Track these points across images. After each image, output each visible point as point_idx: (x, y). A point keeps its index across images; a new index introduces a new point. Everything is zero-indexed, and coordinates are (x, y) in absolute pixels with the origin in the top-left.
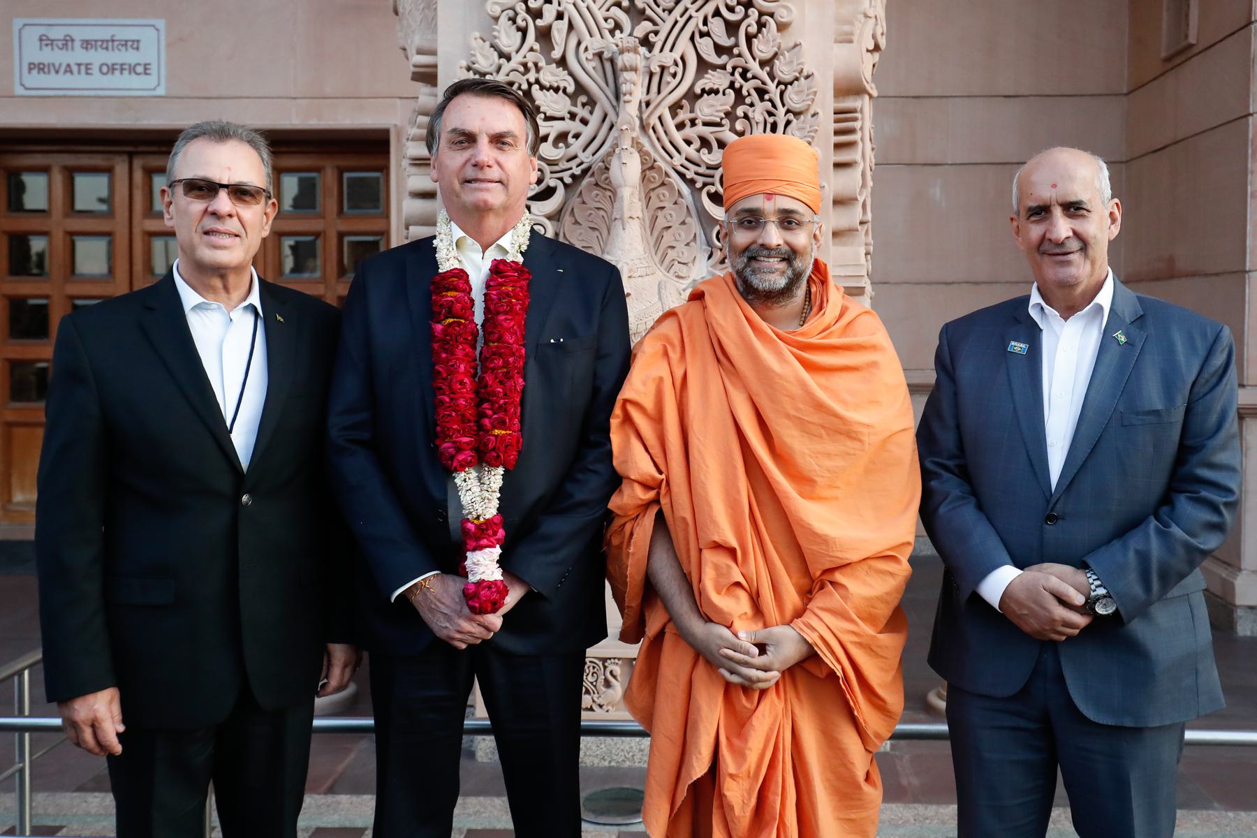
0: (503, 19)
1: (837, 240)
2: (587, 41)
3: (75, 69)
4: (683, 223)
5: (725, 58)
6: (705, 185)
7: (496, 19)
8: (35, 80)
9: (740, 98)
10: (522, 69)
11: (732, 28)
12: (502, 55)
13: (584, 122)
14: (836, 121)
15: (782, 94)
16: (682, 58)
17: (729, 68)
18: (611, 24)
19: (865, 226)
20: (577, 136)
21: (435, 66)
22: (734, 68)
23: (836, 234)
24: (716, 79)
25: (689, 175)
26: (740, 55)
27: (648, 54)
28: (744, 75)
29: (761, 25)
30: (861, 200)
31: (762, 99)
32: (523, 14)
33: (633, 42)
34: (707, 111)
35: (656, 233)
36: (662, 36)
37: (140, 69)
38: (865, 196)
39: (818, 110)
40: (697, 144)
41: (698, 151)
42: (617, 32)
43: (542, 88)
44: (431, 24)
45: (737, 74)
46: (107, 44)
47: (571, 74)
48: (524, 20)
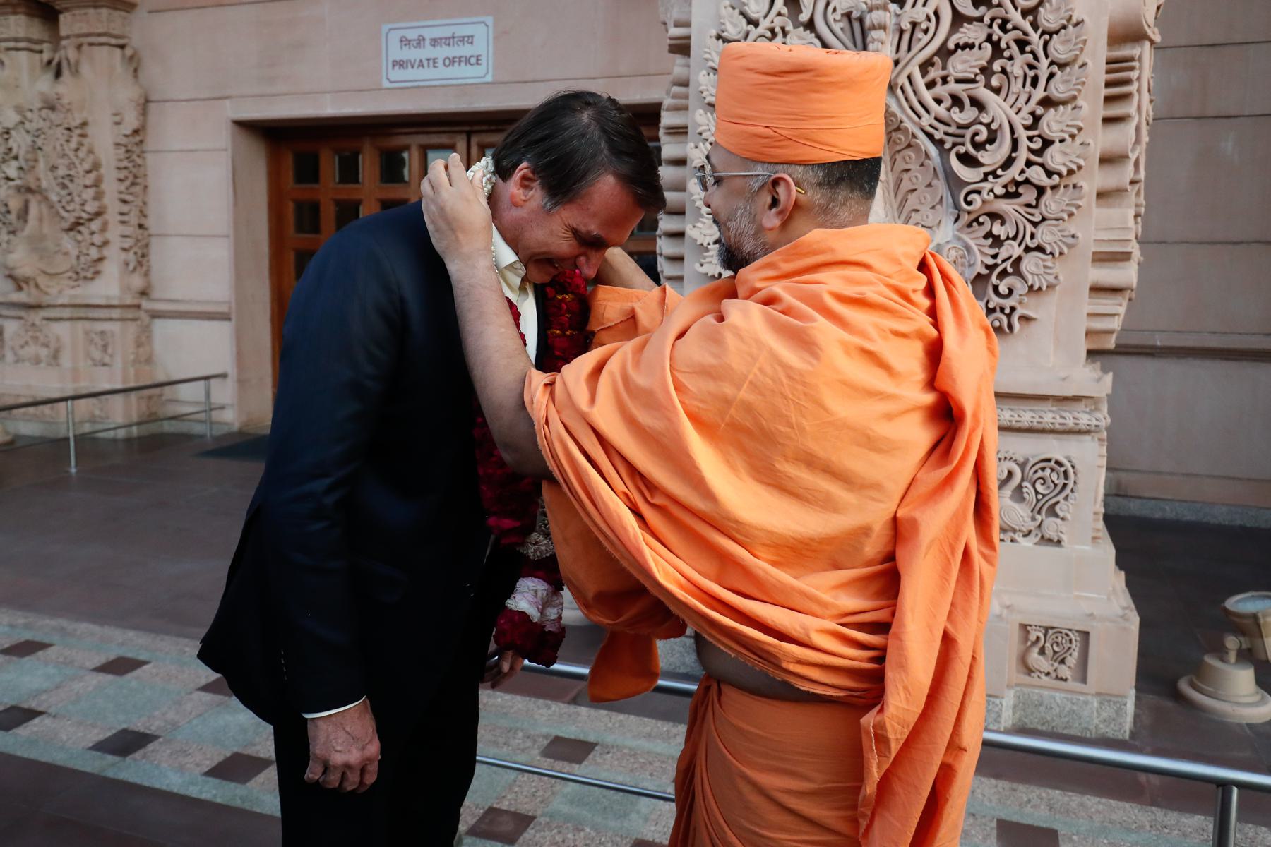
1: (1101, 201)
3: (425, 63)
4: (929, 185)
5: (983, 9)
6: (954, 145)
8: (397, 74)
9: (997, 51)
10: (769, 34)
14: (1108, 72)
16: (936, 13)
17: (987, 20)
19: (1137, 187)
21: (689, 38)
22: (993, 20)
25: (938, 135)
27: (898, 11)
28: (1003, 28)
30: (1133, 157)
31: (1022, 52)
34: (960, 67)
35: (900, 197)
37: (473, 60)
38: (1139, 153)
39: (1087, 60)
40: (948, 102)
41: (949, 110)
45: (995, 27)
46: (449, 41)
47: (818, 37)
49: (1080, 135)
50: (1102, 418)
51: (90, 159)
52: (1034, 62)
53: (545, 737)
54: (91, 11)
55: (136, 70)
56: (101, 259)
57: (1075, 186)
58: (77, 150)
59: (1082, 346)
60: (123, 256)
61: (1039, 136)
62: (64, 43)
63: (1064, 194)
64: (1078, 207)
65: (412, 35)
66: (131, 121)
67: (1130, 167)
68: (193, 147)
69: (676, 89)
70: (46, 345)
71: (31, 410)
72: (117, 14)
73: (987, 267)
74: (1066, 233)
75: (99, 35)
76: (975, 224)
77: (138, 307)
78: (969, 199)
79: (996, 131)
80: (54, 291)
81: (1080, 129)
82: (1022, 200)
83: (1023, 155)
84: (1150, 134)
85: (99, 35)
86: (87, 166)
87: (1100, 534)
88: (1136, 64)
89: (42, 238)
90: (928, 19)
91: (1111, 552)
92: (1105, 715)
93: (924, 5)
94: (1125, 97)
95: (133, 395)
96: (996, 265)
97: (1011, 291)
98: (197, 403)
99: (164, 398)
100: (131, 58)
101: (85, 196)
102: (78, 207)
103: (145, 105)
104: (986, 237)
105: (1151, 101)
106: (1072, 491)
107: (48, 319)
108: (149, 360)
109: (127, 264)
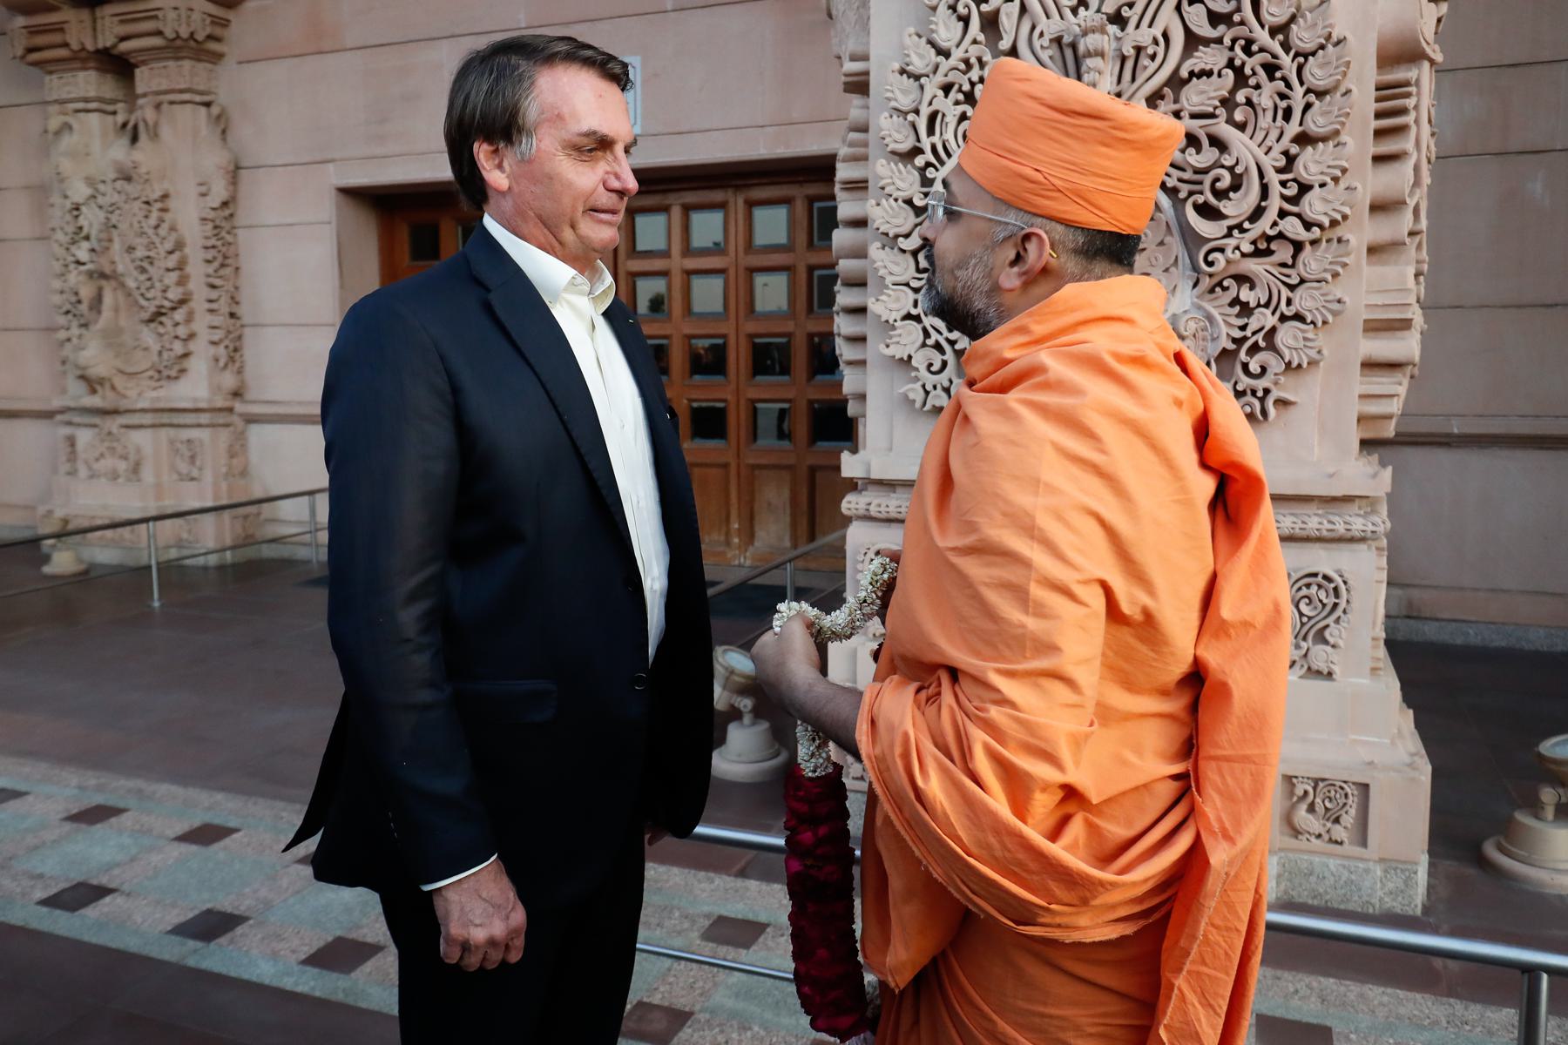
0: (942, 10)
1: (1374, 258)
4: (1161, 243)
5: (1222, 28)
6: (1191, 193)
7: (934, 9)
9: (1241, 79)
10: (963, 66)
14: (1377, 100)
15: (1300, 69)
16: (1165, 35)
17: (1227, 41)
19: (1417, 239)
21: (867, 73)
22: (1234, 41)
23: (1372, 250)
26: (1242, 23)
27: (1119, 34)
28: (1247, 50)
30: (1411, 203)
31: (1272, 78)
34: (1195, 99)
38: (1420, 197)
41: (1183, 151)
42: (1082, 9)
44: (864, 24)
45: (1238, 49)
48: (967, 6)
49: (1345, 175)
50: (1381, 522)
51: (173, 237)
52: (1287, 91)
53: (707, 916)
54: (171, 63)
55: (224, 132)
56: (186, 355)
57: (1339, 240)
58: (157, 227)
59: (1354, 436)
60: (212, 350)
61: (1294, 180)
62: (141, 102)
63: (1326, 250)
64: (1345, 265)
66: (219, 192)
67: (1408, 215)
68: (289, 221)
69: (854, 136)
70: (125, 458)
71: (109, 533)
72: (201, 66)
73: (1234, 340)
74: (1330, 298)
75: (181, 91)
76: (1218, 289)
77: (230, 410)
78: (1210, 258)
79: (1241, 175)
80: (132, 393)
81: (1344, 171)
82: (1275, 258)
83: (1275, 204)
84: (1432, 174)
85: (181, 91)
86: (169, 246)
87: (1381, 665)
88: (1413, 89)
89: (119, 331)
90: (1156, 42)
91: (1396, 685)
92: (1390, 885)
93: (1150, 26)
94: (1401, 130)
95: (226, 515)
96: (1245, 339)
97: (1264, 369)
98: (300, 523)
99: (262, 517)
100: (219, 117)
101: (167, 282)
102: (159, 294)
103: (235, 172)
104: (1232, 304)
105: (1433, 135)
106: (1345, 612)
107: (127, 427)
108: (244, 473)
109: (217, 360)
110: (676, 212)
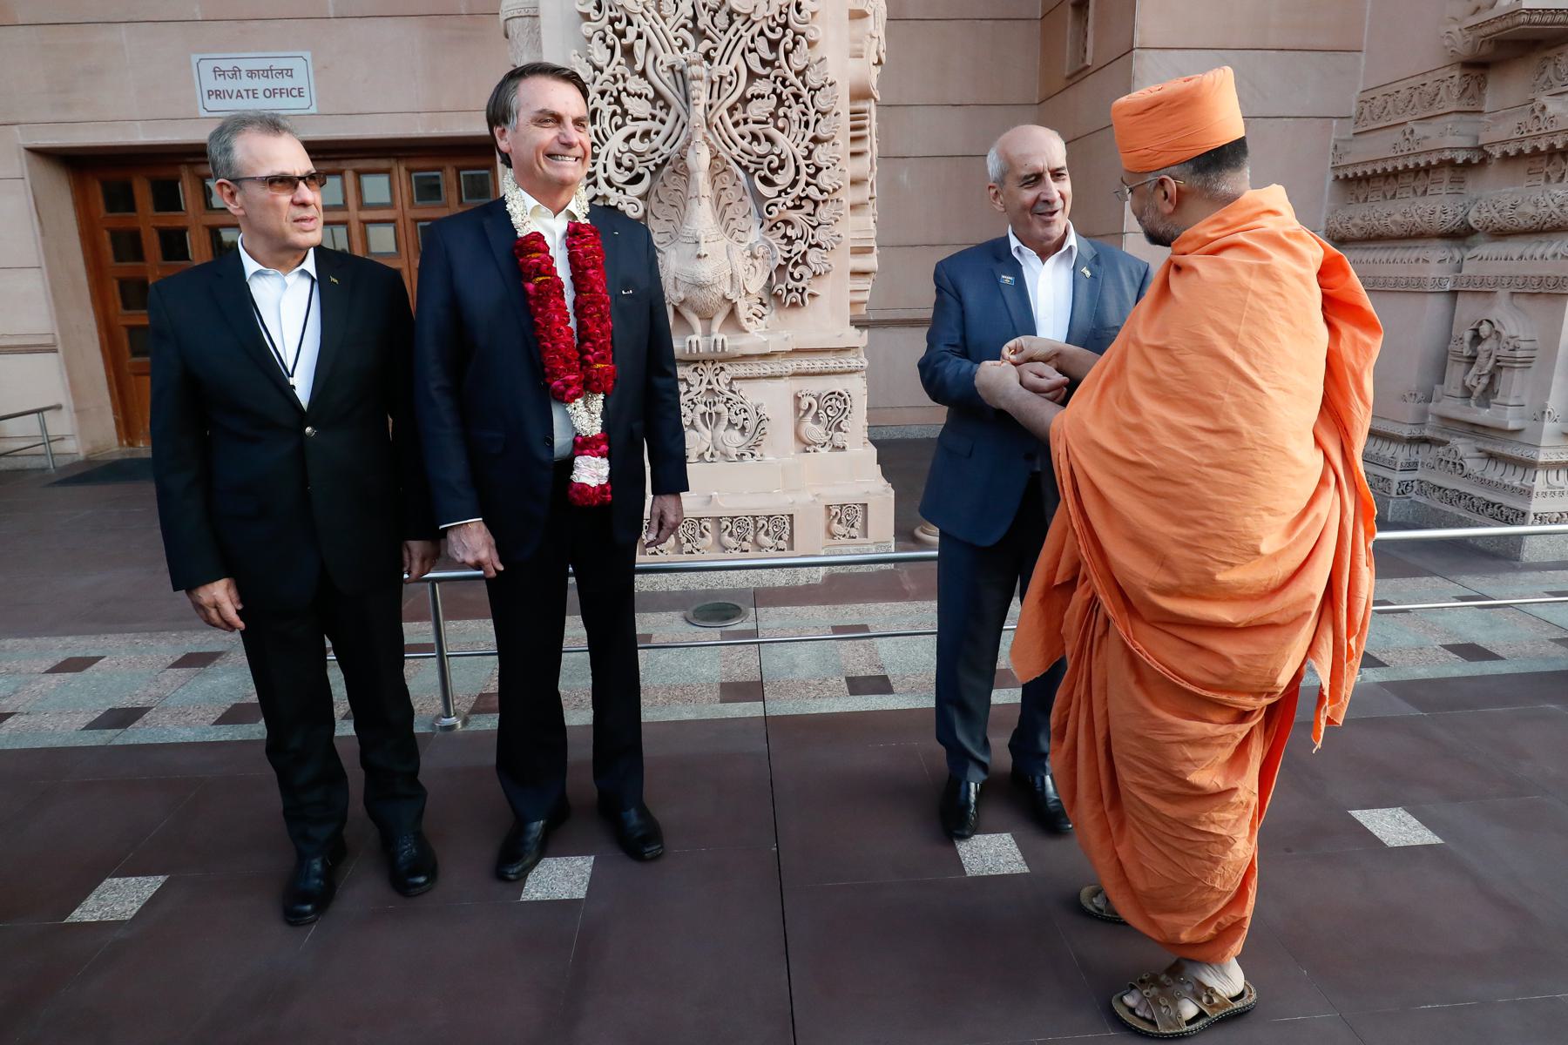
0: (595, 39)
2: (662, 57)
5: (768, 69)
7: (590, 39)
8: (213, 103)
9: (781, 102)
11: (773, 45)
12: (596, 68)
13: (663, 122)
18: (680, 42)
20: (657, 133)
23: (853, 207)
24: (762, 87)
28: (783, 83)
29: (796, 43)
32: (611, 35)
33: (698, 56)
36: (720, 51)
37: (295, 93)
40: (749, 138)
43: (629, 94)
46: (268, 73)
59: (847, 314)
65: (226, 65)
83: (803, 178)
110: (349, 176)
